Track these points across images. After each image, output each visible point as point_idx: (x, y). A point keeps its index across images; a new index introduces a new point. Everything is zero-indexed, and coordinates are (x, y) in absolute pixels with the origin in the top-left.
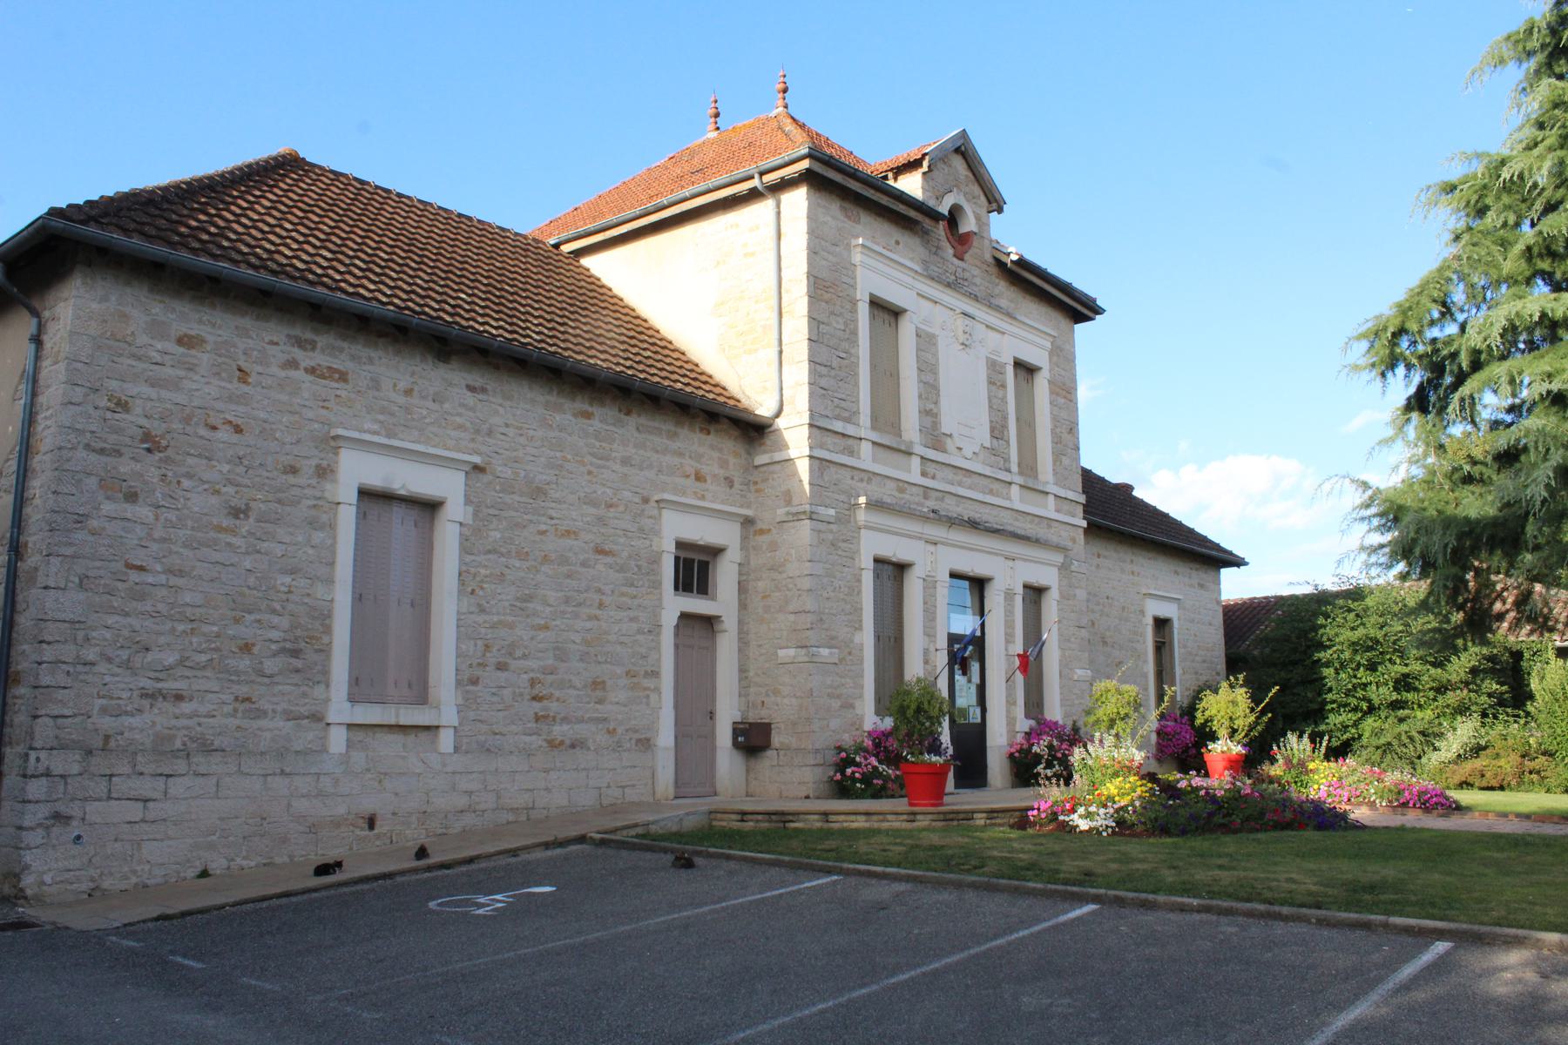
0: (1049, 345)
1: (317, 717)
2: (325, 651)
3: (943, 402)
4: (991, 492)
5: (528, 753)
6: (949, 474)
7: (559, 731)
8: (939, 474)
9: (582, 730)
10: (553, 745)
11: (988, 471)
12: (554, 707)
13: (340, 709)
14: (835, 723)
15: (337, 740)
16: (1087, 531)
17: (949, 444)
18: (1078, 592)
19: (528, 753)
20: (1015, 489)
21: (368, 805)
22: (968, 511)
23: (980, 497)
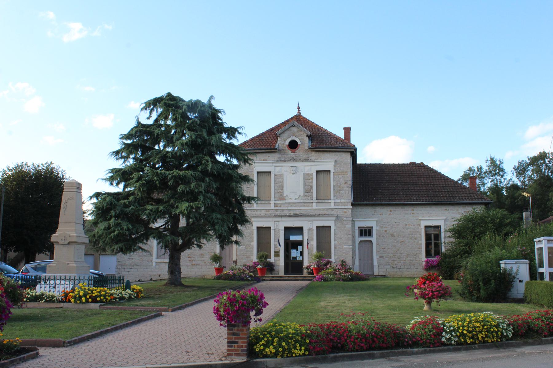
0: (333, 163)
1: (151, 261)
2: (153, 252)
3: (284, 188)
4: (304, 206)
5: (187, 266)
6: (287, 205)
7: (194, 262)
8: (282, 206)
9: (199, 262)
10: (192, 265)
11: (302, 201)
12: (193, 259)
13: (154, 259)
14: (244, 261)
15: (154, 264)
16: (352, 209)
17: (287, 198)
18: (347, 226)
19: (187, 266)
20: (314, 204)
21: (159, 273)
22: (292, 213)
23: (298, 208)
